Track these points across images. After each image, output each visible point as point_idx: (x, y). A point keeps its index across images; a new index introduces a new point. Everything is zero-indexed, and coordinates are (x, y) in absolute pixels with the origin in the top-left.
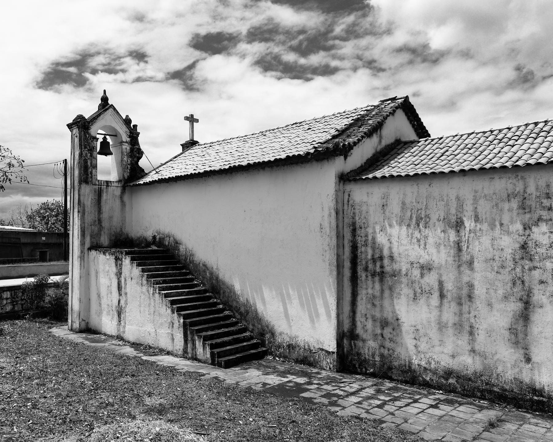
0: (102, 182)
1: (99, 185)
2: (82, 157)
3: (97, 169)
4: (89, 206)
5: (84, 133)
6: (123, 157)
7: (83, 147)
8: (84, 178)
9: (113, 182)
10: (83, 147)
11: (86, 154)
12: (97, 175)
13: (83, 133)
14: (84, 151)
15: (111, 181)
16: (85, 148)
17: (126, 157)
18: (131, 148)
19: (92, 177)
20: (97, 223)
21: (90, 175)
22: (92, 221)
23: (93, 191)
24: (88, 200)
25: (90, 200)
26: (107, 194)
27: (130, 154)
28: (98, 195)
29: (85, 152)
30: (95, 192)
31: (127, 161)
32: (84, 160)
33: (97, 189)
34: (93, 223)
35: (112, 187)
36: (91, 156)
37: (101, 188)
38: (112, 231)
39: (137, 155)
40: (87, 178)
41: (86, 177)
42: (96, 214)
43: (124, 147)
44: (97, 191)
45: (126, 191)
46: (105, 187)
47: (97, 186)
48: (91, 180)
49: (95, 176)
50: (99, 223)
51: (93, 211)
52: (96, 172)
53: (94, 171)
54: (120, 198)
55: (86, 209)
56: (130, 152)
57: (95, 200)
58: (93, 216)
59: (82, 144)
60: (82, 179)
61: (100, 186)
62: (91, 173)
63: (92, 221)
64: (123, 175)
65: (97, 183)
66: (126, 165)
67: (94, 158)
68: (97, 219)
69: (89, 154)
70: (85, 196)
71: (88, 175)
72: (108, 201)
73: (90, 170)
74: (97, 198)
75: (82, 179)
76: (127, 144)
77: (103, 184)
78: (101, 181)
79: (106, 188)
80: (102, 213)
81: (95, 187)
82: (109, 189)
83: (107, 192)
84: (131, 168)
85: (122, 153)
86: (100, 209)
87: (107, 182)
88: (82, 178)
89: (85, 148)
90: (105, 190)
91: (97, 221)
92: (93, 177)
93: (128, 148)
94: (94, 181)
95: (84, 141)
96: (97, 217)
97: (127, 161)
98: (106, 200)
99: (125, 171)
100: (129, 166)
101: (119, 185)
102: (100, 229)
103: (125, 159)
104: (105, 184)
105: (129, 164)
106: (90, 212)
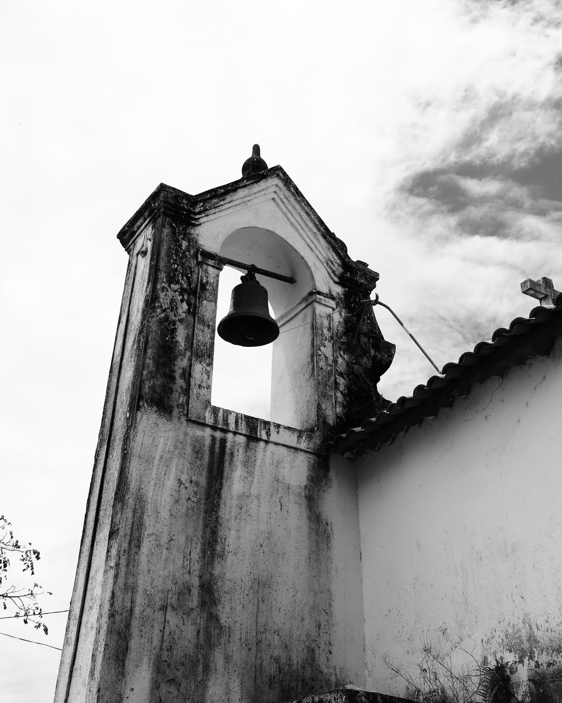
0: (232, 420)
1: (214, 428)
2: (154, 309)
3: (210, 364)
4: (164, 514)
5: (174, 233)
6: (317, 342)
7: (162, 276)
8: (152, 388)
9: (278, 426)
10: (162, 276)
11: (172, 301)
12: (209, 387)
13: (166, 231)
14: (163, 289)
15: (266, 423)
16: (171, 280)
17: (329, 345)
18: (347, 321)
19: (187, 391)
20: (194, 601)
21: (180, 382)
22: (169, 585)
23: (189, 450)
24: (160, 484)
25: (171, 483)
26: (251, 473)
27: (344, 339)
28: (210, 469)
29: (170, 293)
30: (197, 452)
31: (335, 361)
32: (161, 322)
33: (208, 442)
34: (173, 600)
35: (271, 447)
36: (193, 311)
37: (223, 441)
38: (266, 657)
39: (372, 352)
40: (167, 390)
41: (163, 386)
42: (195, 556)
43: (320, 310)
44: (207, 449)
45: (332, 475)
46: (241, 439)
47: (208, 431)
48: (182, 399)
49: (203, 391)
50: (203, 604)
51: (181, 540)
52: (209, 374)
53: (198, 368)
54: (304, 502)
55: (148, 521)
56: (345, 333)
57: (192, 488)
58: (180, 563)
59: (162, 264)
60: (146, 389)
61: (218, 435)
62: (187, 375)
63: (169, 585)
64: (319, 407)
65: (209, 420)
66: (330, 373)
67: (203, 321)
68: (196, 581)
69: (185, 306)
70: (149, 460)
71: (173, 379)
72: (253, 506)
73: (182, 363)
74: (203, 481)
75: (146, 389)
76: (332, 303)
77: (232, 427)
78: (227, 413)
79: (247, 447)
80: (222, 556)
81: (198, 432)
82: (260, 455)
83: (248, 463)
84: (348, 387)
85: (314, 327)
86: (214, 533)
87: (252, 422)
88: (147, 385)
89: (171, 280)
90: (240, 456)
91: (195, 592)
92: (194, 391)
93: (337, 318)
94: (195, 406)
95: (169, 256)
96: (196, 567)
97: (335, 361)
98: (244, 496)
99: (323, 395)
100: (341, 381)
101: (303, 445)
102: (208, 636)
103: (327, 350)
104: (243, 429)
105: (341, 374)
106: (164, 539)
